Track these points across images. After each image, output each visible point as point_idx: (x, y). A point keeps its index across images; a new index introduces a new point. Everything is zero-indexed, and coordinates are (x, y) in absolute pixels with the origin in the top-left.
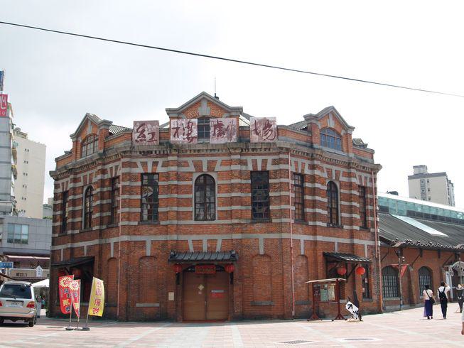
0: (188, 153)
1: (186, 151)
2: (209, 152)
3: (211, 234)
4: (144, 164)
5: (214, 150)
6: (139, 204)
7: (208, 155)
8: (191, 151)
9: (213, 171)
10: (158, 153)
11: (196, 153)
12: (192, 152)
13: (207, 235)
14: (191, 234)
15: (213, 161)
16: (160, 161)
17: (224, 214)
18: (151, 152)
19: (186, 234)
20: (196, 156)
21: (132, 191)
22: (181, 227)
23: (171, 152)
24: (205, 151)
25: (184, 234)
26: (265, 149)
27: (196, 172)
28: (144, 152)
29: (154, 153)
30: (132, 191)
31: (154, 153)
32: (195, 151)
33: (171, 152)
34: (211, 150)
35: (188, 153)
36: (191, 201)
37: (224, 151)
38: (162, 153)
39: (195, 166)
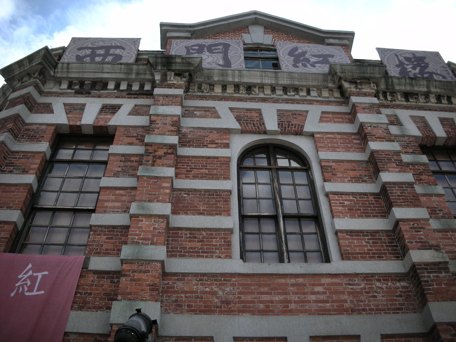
0: (218, 90)
1: (212, 86)
2: (279, 92)
3: (323, 312)
4: (75, 110)
5: (297, 90)
6: (22, 195)
7: (276, 101)
8: (224, 88)
9: (299, 133)
10: (123, 86)
11: (243, 93)
12: (230, 90)
13: (302, 319)
14: (229, 312)
15: (295, 113)
16: (128, 104)
17: (365, 244)
18: (104, 85)
19: (208, 310)
20: (240, 100)
21: (11, 164)
22: (179, 285)
23: (164, 77)
24: (268, 91)
25: (192, 311)
26: (439, 98)
27: (243, 132)
28: (82, 83)
29: (111, 86)
30: (11, 164)
31: (111, 86)
32: (237, 86)
33: (164, 77)
34: (285, 89)
35: (218, 90)
36: (227, 201)
37: (325, 94)
38: (136, 87)
39: (238, 119)
